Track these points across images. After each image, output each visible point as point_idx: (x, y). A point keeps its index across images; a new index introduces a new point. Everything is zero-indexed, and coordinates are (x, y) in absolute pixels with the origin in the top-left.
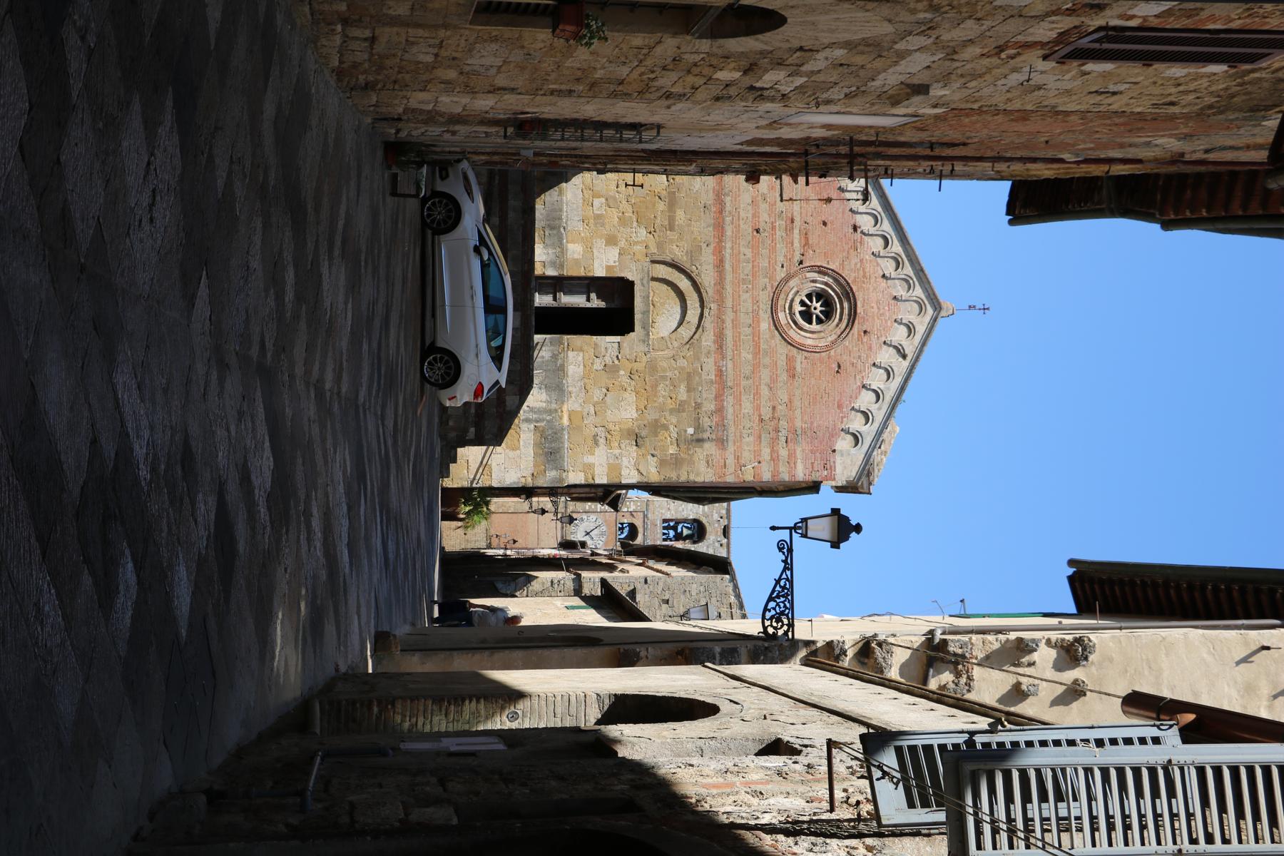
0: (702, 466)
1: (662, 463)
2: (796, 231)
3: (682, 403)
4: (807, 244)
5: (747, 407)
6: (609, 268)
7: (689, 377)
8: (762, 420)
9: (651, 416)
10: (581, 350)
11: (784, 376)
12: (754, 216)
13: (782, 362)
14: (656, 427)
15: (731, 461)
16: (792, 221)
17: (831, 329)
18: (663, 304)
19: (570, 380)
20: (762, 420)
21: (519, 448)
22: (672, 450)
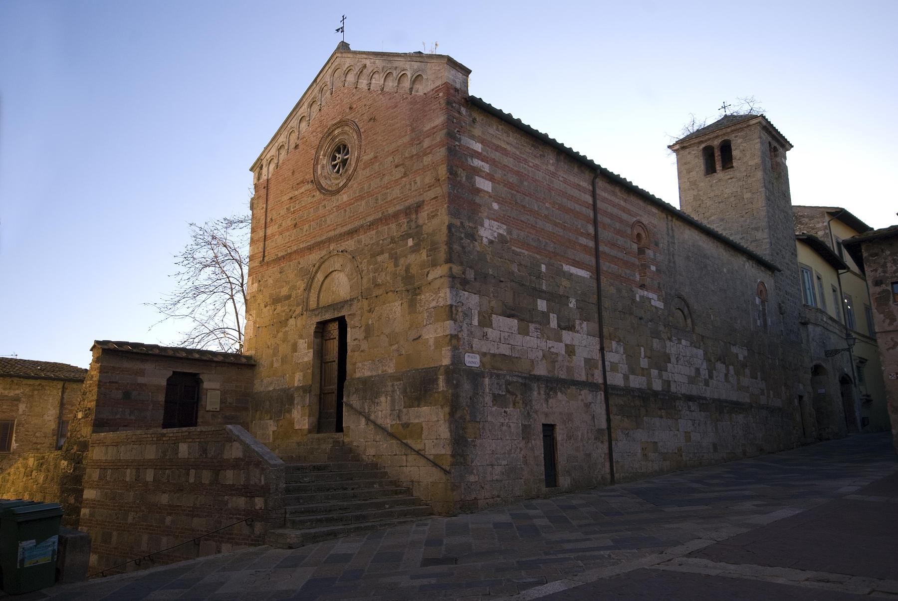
0: (436, 221)
1: (434, 264)
2: (296, 193)
3: (391, 257)
4: (302, 182)
5: (396, 192)
6: (309, 348)
7: (374, 256)
8: (405, 175)
9: (401, 287)
10: (355, 364)
11: (376, 166)
12: (288, 230)
13: (367, 172)
14: (408, 278)
15: (431, 194)
16: (291, 198)
17: (352, 139)
18: (333, 292)
19: (374, 373)
20: (405, 175)
21: (421, 424)
22: (424, 255)
